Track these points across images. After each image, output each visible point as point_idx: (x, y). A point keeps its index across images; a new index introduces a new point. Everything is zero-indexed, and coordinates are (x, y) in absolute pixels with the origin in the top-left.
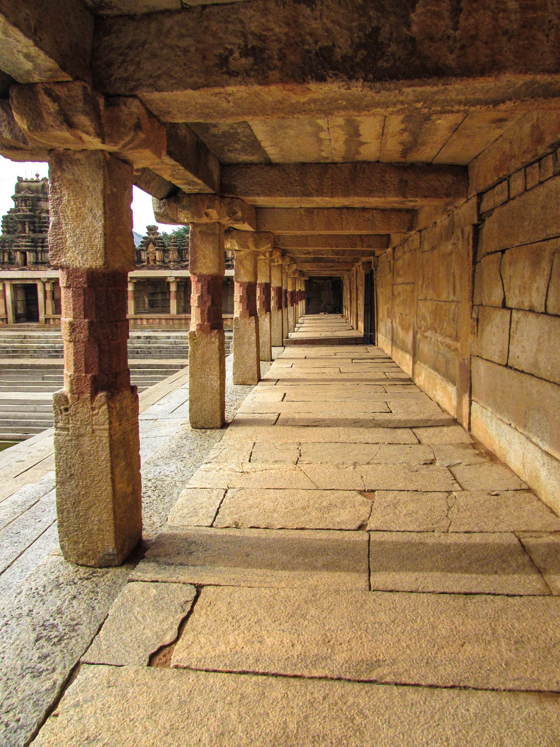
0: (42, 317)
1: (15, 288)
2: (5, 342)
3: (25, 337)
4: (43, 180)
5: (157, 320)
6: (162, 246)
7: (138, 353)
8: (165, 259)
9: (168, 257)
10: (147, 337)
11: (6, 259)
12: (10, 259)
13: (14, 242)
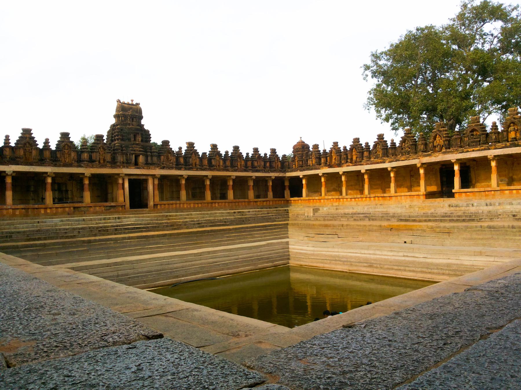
0: (151, 203)
1: (130, 181)
2: (157, 220)
10: (239, 212)
12: (127, 160)
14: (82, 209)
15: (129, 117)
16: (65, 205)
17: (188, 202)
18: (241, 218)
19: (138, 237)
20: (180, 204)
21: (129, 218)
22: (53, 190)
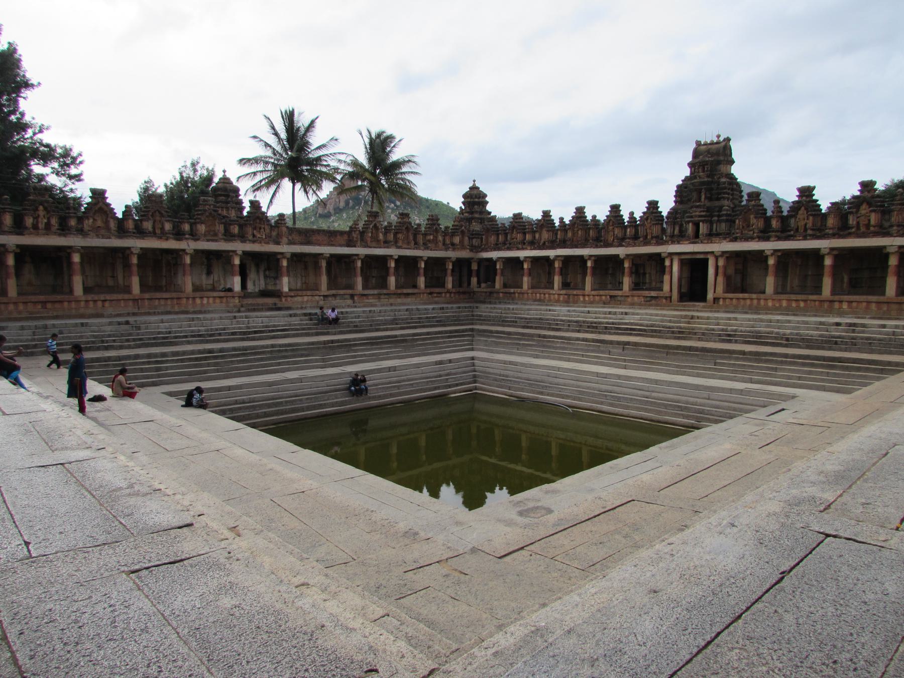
0: (710, 296)
1: (682, 263)
2: (670, 321)
3: (692, 317)
4: (724, 140)
5: (864, 304)
6: (881, 206)
7: (836, 343)
8: (884, 222)
9: (889, 220)
10: (850, 325)
11: (676, 232)
12: (681, 231)
13: (685, 212)
14: (619, 298)
15: (712, 161)
16: (601, 292)
17: (775, 297)
18: (839, 337)
19: (594, 341)
20: (759, 299)
21: (638, 314)
22: (631, 273)
